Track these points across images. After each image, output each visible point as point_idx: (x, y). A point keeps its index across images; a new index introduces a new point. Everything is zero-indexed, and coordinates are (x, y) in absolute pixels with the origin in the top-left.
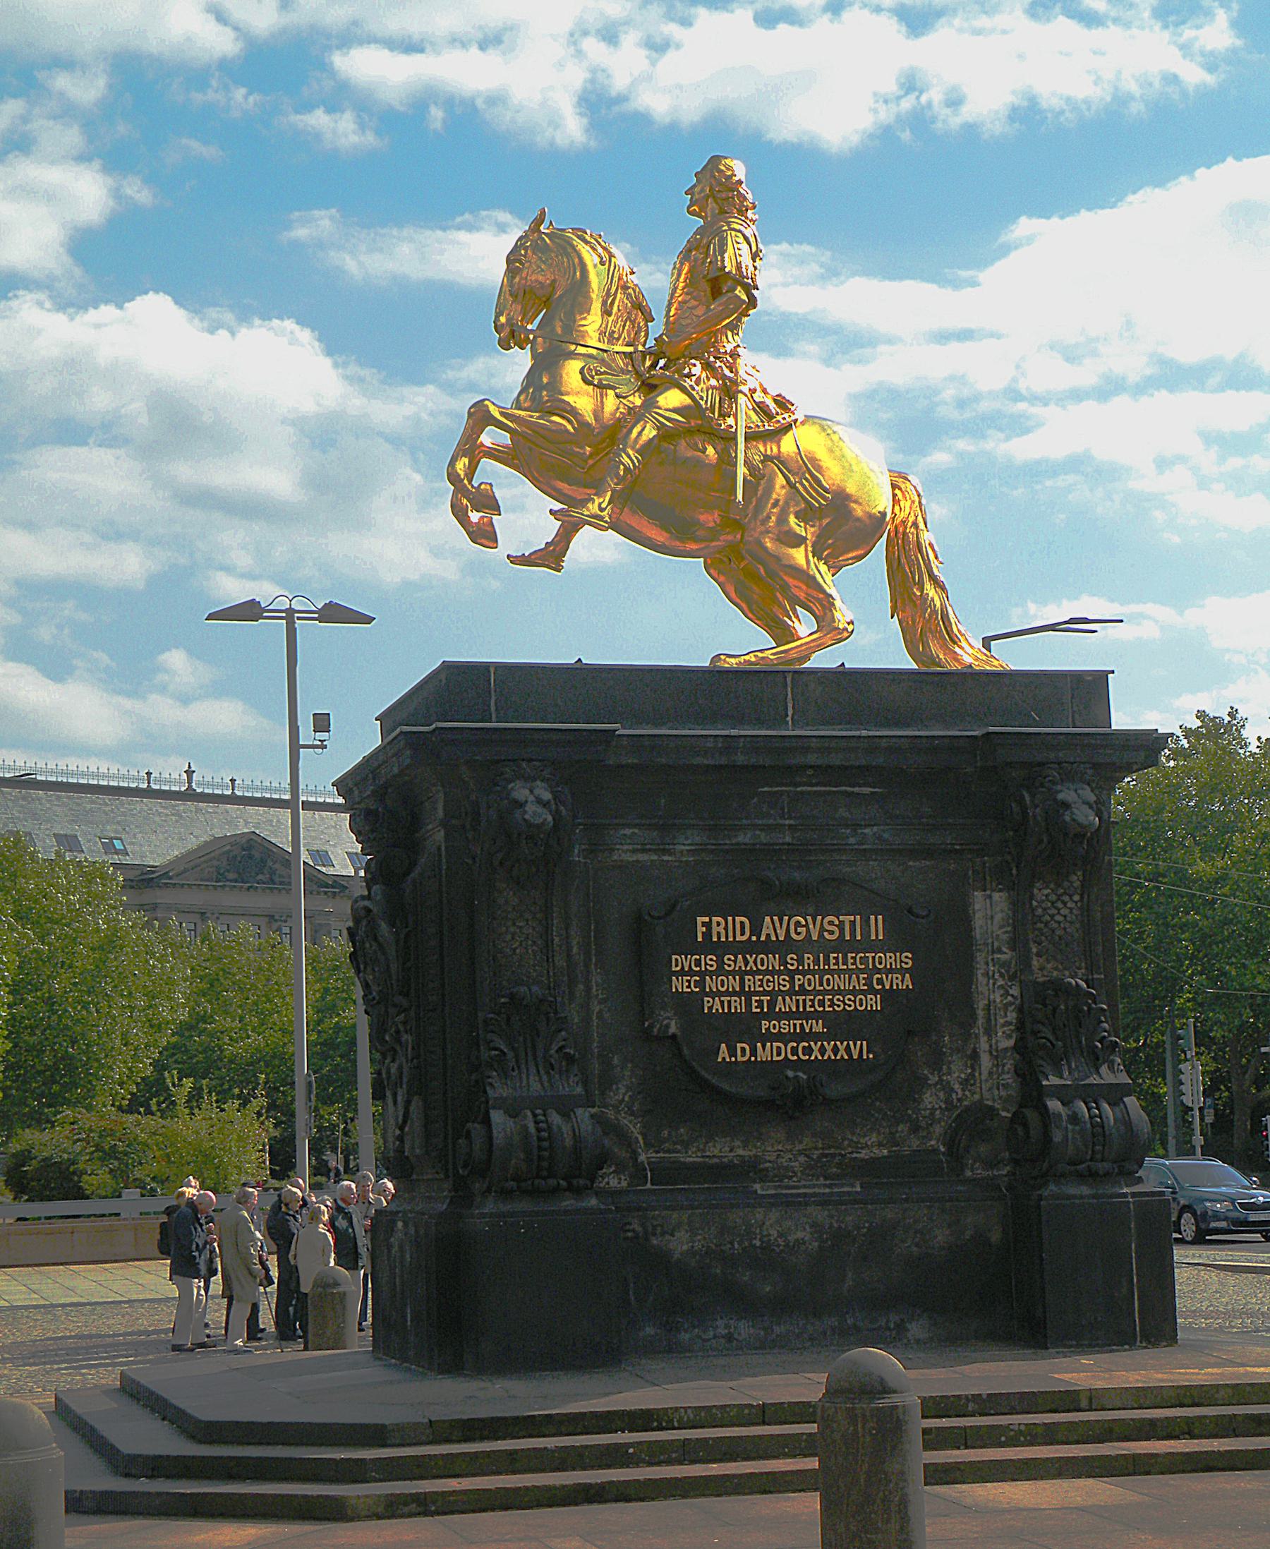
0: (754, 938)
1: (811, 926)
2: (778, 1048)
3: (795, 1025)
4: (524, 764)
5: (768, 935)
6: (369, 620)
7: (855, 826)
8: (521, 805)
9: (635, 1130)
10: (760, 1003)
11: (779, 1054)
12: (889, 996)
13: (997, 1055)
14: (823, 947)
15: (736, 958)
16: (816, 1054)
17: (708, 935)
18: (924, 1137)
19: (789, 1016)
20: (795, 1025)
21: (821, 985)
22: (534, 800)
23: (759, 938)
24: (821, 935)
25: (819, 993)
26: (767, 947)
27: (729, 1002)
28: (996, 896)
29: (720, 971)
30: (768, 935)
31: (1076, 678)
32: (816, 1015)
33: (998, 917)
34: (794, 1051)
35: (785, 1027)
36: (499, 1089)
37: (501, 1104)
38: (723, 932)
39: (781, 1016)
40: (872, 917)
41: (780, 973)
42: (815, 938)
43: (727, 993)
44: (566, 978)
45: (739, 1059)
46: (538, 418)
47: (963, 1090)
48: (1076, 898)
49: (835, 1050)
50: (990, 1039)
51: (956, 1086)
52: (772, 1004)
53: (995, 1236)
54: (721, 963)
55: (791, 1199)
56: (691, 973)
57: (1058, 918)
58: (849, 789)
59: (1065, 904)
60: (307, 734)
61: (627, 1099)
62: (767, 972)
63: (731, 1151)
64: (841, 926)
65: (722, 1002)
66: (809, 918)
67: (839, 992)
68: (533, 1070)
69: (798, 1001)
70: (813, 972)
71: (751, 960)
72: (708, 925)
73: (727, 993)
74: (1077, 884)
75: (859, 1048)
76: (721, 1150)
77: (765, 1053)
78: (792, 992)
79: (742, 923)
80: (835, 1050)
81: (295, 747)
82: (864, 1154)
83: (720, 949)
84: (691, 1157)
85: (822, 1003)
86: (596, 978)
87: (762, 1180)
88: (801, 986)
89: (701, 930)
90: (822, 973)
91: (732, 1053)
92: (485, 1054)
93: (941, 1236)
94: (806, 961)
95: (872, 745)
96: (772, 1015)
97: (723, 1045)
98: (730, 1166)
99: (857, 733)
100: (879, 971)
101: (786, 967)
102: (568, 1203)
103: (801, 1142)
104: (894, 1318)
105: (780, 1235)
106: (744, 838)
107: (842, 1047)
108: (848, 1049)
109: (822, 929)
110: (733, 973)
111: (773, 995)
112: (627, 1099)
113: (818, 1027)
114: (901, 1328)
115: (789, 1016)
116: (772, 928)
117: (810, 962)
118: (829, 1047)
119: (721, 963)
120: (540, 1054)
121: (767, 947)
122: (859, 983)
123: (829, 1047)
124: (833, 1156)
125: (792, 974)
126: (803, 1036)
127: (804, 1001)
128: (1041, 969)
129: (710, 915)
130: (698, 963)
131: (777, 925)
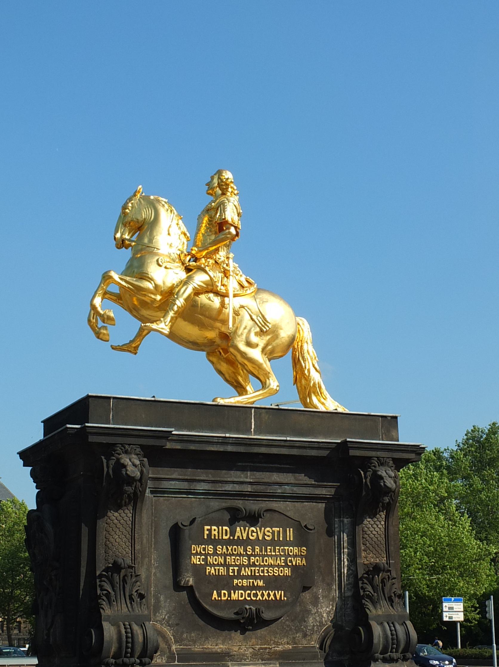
0: (231, 538)
1: (259, 533)
2: (242, 593)
3: (250, 582)
4: (127, 447)
5: (238, 537)
9: (169, 633)
10: (234, 570)
11: (242, 597)
12: (295, 568)
14: (263, 543)
15: (223, 547)
16: (259, 597)
18: (309, 640)
19: (247, 577)
20: (250, 582)
21: (263, 562)
22: (132, 464)
23: (234, 537)
24: (263, 537)
25: (262, 566)
26: (239, 542)
27: (219, 570)
28: (346, 520)
29: (215, 553)
30: (238, 537)
32: (260, 578)
34: (249, 595)
35: (245, 582)
36: (107, 611)
37: (108, 619)
38: (217, 534)
39: (243, 577)
40: (288, 529)
41: (243, 556)
43: (218, 565)
44: (140, 556)
45: (223, 598)
46: (136, 281)
47: (328, 617)
48: (383, 523)
49: (269, 595)
51: (325, 615)
52: (239, 571)
54: (215, 549)
57: (374, 532)
58: (279, 466)
59: (377, 525)
61: (166, 617)
62: (237, 555)
63: (216, 646)
65: (215, 570)
66: (258, 528)
67: (271, 566)
69: (251, 570)
71: (230, 549)
72: (210, 530)
73: (218, 565)
74: (383, 516)
75: (280, 594)
77: (234, 596)
78: (249, 566)
79: (226, 530)
80: (269, 595)
83: (215, 542)
84: (197, 648)
85: (263, 571)
86: (154, 556)
87: (231, 661)
88: (254, 562)
89: (206, 532)
91: (219, 595)
94: (256, 550)
95: (292, 445)
96: (239, 576)
97: (215, 592)
99: (285, 439)
100: (290, 556)
101: (246, 553)
103: (250, 642)
106: (229, 487)
107: (272, 594)
108: (275, 594)
110: (221, 555)
111: (240, 566)
112: (166, 617)
113: (261, 583)
115: (247, 577)
116: (240, 532)
117: (258, 550)
119: (215, 549)
120: (127, 594)
121: (239, 542)
123: (266, 594)
124: (266, 648)
126: (253, 587)
127: (255, 570)
130: (204, 549)
131: (243, 531)
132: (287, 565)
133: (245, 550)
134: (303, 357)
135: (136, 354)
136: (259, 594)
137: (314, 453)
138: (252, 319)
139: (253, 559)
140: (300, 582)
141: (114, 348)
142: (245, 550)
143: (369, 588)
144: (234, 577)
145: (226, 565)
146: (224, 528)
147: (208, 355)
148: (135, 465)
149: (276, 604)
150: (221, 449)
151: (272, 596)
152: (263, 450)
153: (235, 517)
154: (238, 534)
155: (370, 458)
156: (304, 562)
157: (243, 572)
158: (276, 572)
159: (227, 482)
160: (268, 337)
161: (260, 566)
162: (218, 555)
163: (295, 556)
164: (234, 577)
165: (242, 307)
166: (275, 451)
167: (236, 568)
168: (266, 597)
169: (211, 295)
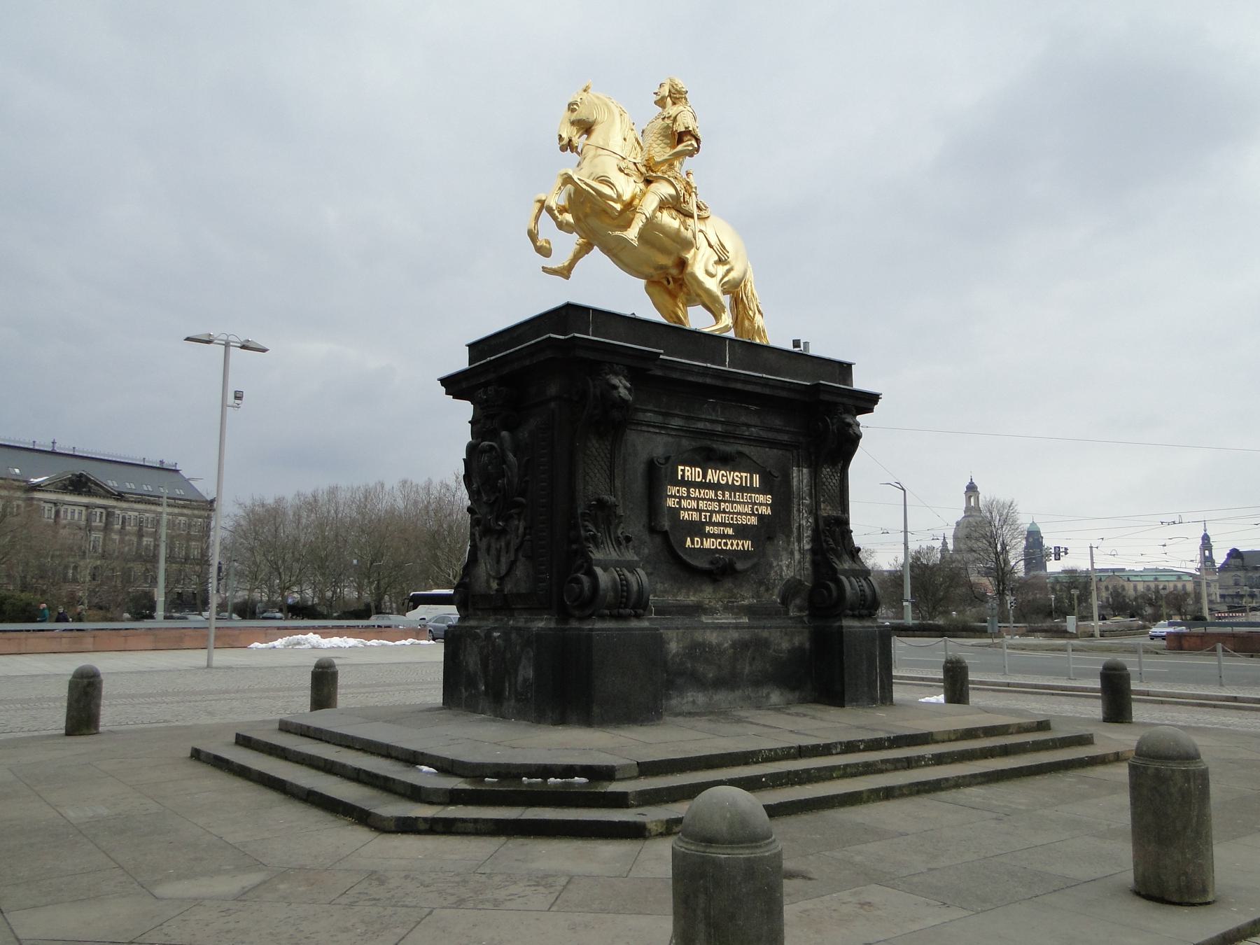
6: (264, 350)
7: (749, 426)
8: (615, 387)
12: (761, 517)
17: (683, 476)
22: (622, 387)
26: (710, 486)
28: (805, 470)
29: (688, 497)
31: (840, 364)
32: (729, 525)
35: (716, 530)
52: (711, 517)
53: (807, 645)
54: (688, 492)
55: (720, 624)
56: (675, 497)
62: (709, 500)
72: (683, 471)
75: (747, 544)
77: (708, 544)
78: (719, 512)
81: (224, 405)
82: (746, 602)
83: (689, 484)
89: (680, 473)
90: (733, 502)
91: (693, 543)
93: (785, 645)
98: (688, 606)
102: (634, 624)
104: (765, 692)
106: (700, 425)
110: (694, 499)
111: (712, 512)
113: (730, 531)
114: (768, 696)
116: (713, 476)
119: (688, 492)
121: (710, 486)
122: (747, 509)
125: (720, 501)
132: (753, 514)
133: (716, 495)
135: (567, 277)
137: (784, 394)
140: (766, 532)
141: (545, 269)
142: (716, 495)
143: (831, 542)
145: (698, 510)
148: (626, 387)
149: (743, 554)
150: (700, 380)
152: (739, 386)
153: (708, 458)
155: (836, 404)
156: (769, 511)
158: (744, 520)
159: (700, 420)
160: (727, 267)
161: (729, 513)
163: (761, 504)
164: (706, 523)
165: (701, 231)
166: (749, 388)
169: (674, 213)
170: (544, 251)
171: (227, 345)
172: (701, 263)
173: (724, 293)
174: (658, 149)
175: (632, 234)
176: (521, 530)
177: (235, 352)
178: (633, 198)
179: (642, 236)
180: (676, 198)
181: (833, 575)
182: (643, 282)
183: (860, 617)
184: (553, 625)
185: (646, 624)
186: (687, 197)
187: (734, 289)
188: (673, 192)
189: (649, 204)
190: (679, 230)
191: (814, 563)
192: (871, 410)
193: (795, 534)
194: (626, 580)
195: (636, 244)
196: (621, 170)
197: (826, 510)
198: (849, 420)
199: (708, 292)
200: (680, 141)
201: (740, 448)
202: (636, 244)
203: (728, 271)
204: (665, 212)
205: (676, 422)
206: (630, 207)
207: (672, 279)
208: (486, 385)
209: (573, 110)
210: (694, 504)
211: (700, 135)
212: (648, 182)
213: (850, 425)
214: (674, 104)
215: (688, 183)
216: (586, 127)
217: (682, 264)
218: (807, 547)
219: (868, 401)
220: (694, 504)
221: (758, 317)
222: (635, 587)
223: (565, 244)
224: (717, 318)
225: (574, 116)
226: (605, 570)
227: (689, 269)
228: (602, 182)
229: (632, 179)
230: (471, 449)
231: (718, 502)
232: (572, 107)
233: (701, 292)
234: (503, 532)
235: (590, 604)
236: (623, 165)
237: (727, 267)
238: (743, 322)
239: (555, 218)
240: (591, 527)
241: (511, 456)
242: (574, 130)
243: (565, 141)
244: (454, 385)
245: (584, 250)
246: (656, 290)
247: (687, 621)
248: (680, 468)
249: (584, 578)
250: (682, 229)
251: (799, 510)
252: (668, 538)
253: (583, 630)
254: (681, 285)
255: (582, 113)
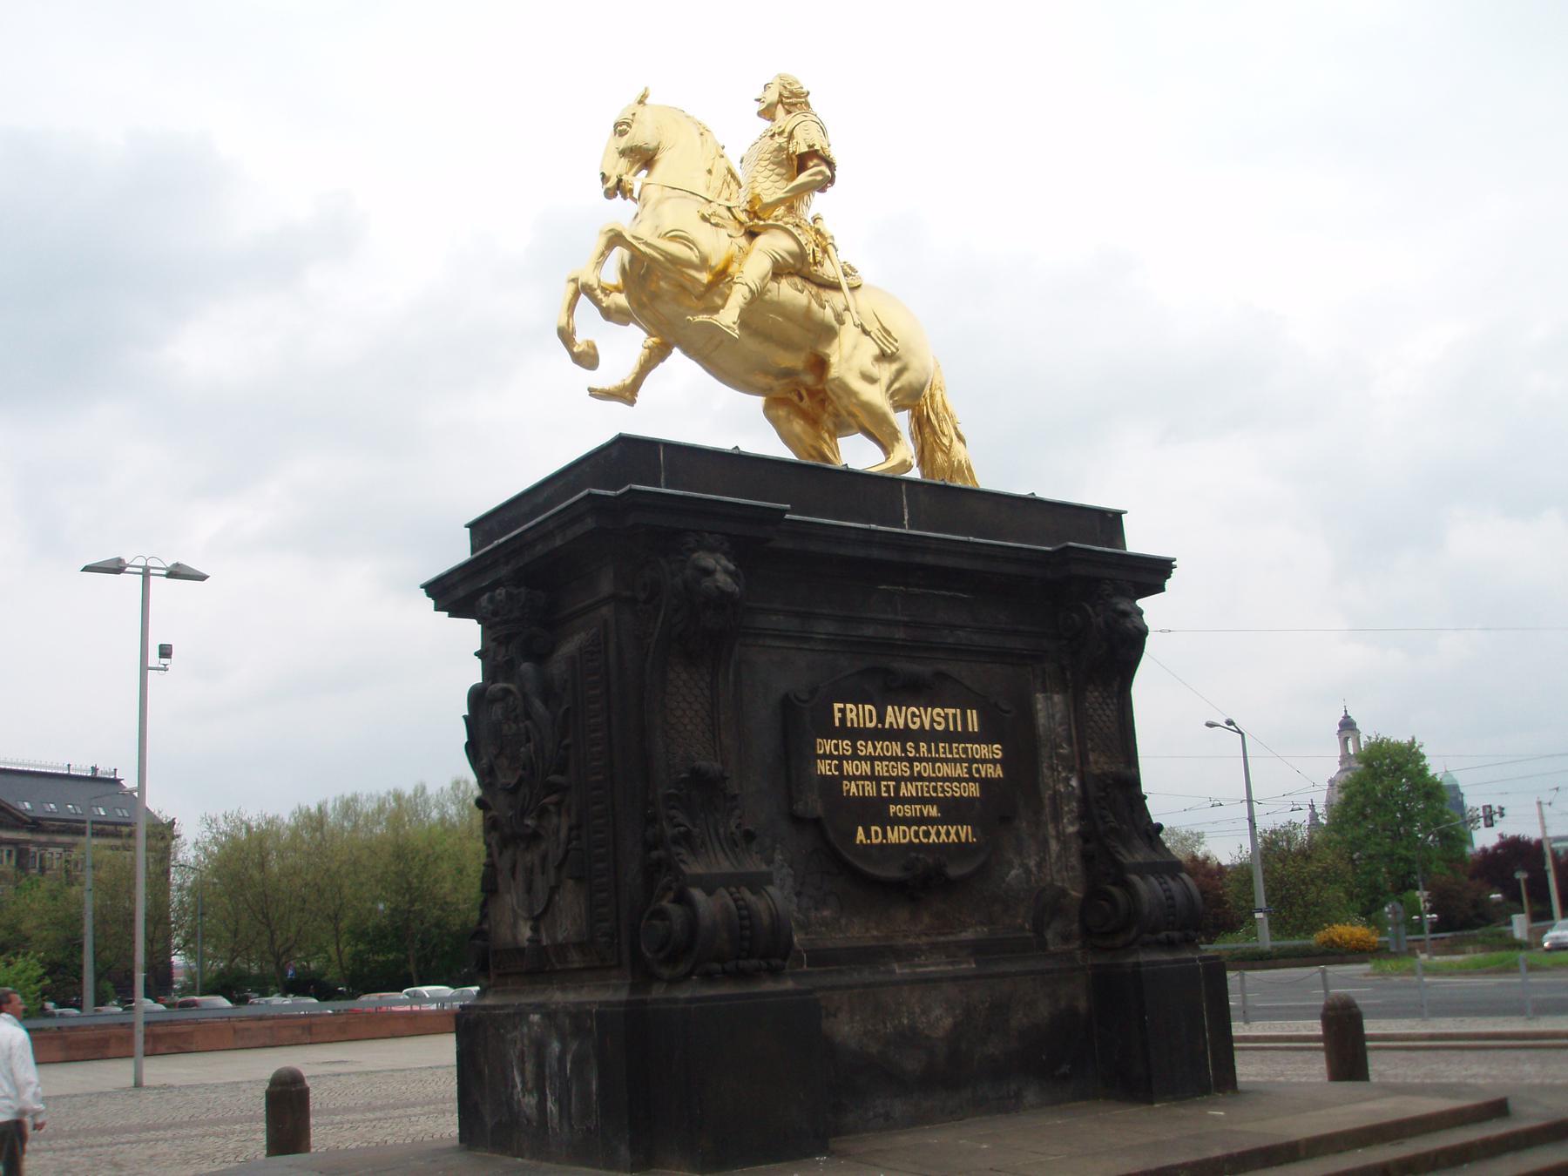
8: (709, 573)
10: (888, 787)
12: (985, 783)
13: (1061, 837)
14: (931, 736)
16: (933, 838)
17: (843, 720)
28: (1057, 698)
29: (855, 756)
33: (1058, 716)
34: (917, 834)
35: (909, 811)
37: (699, 881)
42: (927, 727)
49: (948, 834)
50: (1056, 827)
52: (897, 789)
53: (1082, 1005)
54: (854, 748)
56: (831, 757)
60: (154, 658)
62: (890, 759)
64: (946, 718)
68: (717, 845)
70: (927, 760)
72: (842, 711)
73: (861, 778)
75: (965, 832)
76: (858, 932)
77: (895, 836)
78: (912, 779)
80: (948, 834)
81: (144, 668)
83: (855, 734)
89: (838, 715)
90: (934, 760)
91: (868, 835)
92: (670, 832)
100: (976, 761)
102: (768, 986)
105: (924, 1012)
106: (869, 631)
107: (953, 831)
108: (957, 834)
109: (933, 720)
110: (865, 758)
116: (896, 717)
118: (943, 830)
119: (854, 748)
122: (960, 771)
123: (943, 830)
125: (911, 761)
128: (1096, 762)
129: (845, 702)
132: (972, 779)
134: (937, 415)
135: (632, 402)
136: (933, 831)
138: (866, 332)
139: (917, 767)
140: (998, 809)
141: (593, 393)
142: (904, 750)
144: (890, 801)
145: (873, 778)
146: (867, 707)
147: (767, 409)
148: (726, 571)
149: (960, 848)
150: (861, 553)
151: (953, 837)
152: (930, 559)
154: (889, 719)
156: (998, 772)
157: (903, 791)
160: (895, 367)
161: (930, 779)
162: (860, 759)
163: (984, 761)
164: (890, 801)
166: (949, 562)
167: (892, 784)
168: (943, 836)
169: (797, 280)
170: (587, 359)
171: (146, 574)
172: (850, 359)
173: (898, 407)
174: (768, 184)
175: (728, 317)
176: (563, 833)
177: (159, 584)
178: (729, 262)
179: (744, 322)
180: (801, 256)
181: (1120, 877)
182: (758, 401)
183: (1170, 945)
184: (623, 995)
185: (789, 985)
186: (819, 255)
187: (912, 397)
188: (793, 246)
189: (754, 268)
190: (808, 309)
191: (1087, 858)
192: (1162, 589)
193: (1048, 810)
194: (747, 907)
195: (736, 333)
196: (705, 219)
197: (1099, 763)
198: (1123, 605)
199: (868, 408)
200: (802, 168)
201: (943, 667)
202: (736, 333)
203: (899, 373)
204: (784, 281)
205: (825, 628)
206: (722, 276)
207: (805, 393)
208: (496, 584)
209: (622, 134)
210: (865, 768)
211: (835, 154)
212: (752, 234)
213: (1125, 614)
214: (789, 112)
215: (818, 232)
216: (645, 158)
217: (820, 365)
218: (1071, 829)
219: (1154, 573)
220: (865, 768)
221: (957, 445)
222: (766, 919)
223: (623, 346)
224: (887, 450)
225: (624, 142)
226: (710, 892)
227: (834, 372)
228: (674, 238)
229: (723, 232)
230: (477, 698)
231: (909, 761)
232: (621, 128)
233: (855, 410)
234: (535, 837)
235: (686, 952)
236: (707, 211)
237: (895, 367)
238: (933, 460)
239: (597, 302)
240: (681, 817)
241: (537, 704)
242: (623, 163)
243: (612, 182)
244: (449, 593)
245: (656, 356)
246: (782, 412)
247: (867, 975)
248: (837, 706)
249: (675, 911)
250: (815, 306)
251: (1052, 768)
252: (826, 830)
253: (676, 1001)
254: (822, 402)
255: (640, 135)
